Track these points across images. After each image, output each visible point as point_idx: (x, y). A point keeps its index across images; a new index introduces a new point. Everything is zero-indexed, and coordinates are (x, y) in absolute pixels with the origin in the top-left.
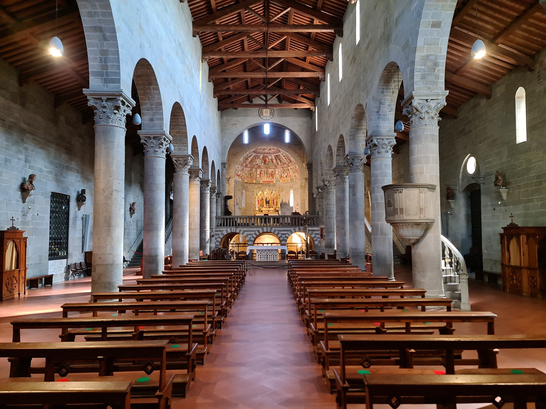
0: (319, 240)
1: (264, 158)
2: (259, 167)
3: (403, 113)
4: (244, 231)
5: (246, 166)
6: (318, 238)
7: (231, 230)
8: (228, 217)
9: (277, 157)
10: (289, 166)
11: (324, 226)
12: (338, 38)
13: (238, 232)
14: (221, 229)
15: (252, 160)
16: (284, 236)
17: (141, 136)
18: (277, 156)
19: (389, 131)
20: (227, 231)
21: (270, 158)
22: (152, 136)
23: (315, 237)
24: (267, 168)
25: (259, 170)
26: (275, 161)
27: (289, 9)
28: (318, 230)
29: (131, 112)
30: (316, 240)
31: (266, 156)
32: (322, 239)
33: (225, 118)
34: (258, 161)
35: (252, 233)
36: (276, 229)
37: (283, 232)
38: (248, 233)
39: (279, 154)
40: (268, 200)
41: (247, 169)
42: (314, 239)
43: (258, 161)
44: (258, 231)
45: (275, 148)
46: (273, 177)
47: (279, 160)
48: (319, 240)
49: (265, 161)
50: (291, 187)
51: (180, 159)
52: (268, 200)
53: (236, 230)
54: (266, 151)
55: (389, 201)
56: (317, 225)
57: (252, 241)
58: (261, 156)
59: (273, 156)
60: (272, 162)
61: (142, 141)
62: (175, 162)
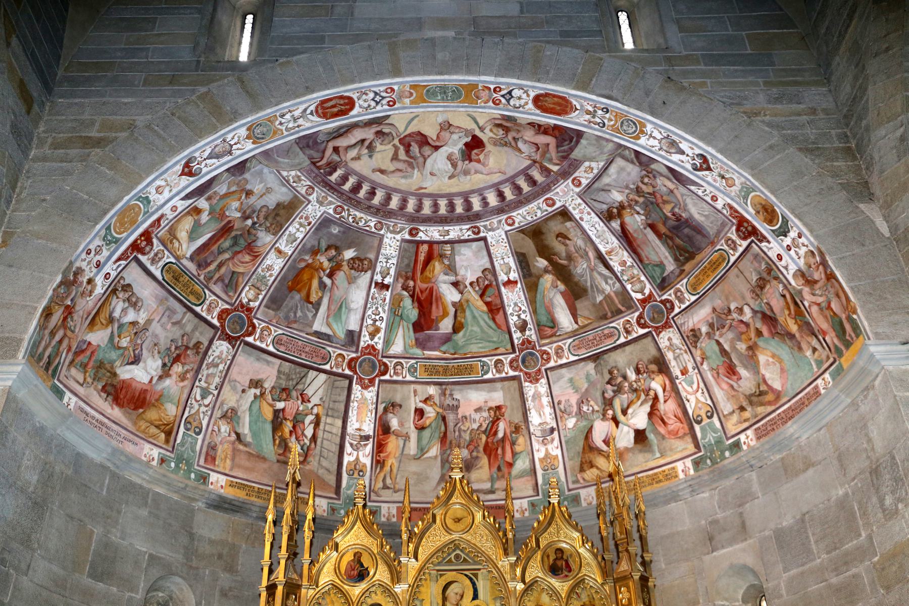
1: (422, 260)
2: (371, 366)
5: (237, 327)
9: (542, 246)
10: (660, 317)
15: (297, 281)
18: (535, 232)
24: (457, 373)
25: (364, 398)
26: (514, 299)
31: (433, 252)
34: (362, 306)
39: (566, 195)
41: (248, 367)
43: (362, 306)
45: (523, 95)
46: (503, 469)
47: (563, 273)
49: (426, 303)
54: (437, 174)
59: (498, 236)
60: (495, 309)
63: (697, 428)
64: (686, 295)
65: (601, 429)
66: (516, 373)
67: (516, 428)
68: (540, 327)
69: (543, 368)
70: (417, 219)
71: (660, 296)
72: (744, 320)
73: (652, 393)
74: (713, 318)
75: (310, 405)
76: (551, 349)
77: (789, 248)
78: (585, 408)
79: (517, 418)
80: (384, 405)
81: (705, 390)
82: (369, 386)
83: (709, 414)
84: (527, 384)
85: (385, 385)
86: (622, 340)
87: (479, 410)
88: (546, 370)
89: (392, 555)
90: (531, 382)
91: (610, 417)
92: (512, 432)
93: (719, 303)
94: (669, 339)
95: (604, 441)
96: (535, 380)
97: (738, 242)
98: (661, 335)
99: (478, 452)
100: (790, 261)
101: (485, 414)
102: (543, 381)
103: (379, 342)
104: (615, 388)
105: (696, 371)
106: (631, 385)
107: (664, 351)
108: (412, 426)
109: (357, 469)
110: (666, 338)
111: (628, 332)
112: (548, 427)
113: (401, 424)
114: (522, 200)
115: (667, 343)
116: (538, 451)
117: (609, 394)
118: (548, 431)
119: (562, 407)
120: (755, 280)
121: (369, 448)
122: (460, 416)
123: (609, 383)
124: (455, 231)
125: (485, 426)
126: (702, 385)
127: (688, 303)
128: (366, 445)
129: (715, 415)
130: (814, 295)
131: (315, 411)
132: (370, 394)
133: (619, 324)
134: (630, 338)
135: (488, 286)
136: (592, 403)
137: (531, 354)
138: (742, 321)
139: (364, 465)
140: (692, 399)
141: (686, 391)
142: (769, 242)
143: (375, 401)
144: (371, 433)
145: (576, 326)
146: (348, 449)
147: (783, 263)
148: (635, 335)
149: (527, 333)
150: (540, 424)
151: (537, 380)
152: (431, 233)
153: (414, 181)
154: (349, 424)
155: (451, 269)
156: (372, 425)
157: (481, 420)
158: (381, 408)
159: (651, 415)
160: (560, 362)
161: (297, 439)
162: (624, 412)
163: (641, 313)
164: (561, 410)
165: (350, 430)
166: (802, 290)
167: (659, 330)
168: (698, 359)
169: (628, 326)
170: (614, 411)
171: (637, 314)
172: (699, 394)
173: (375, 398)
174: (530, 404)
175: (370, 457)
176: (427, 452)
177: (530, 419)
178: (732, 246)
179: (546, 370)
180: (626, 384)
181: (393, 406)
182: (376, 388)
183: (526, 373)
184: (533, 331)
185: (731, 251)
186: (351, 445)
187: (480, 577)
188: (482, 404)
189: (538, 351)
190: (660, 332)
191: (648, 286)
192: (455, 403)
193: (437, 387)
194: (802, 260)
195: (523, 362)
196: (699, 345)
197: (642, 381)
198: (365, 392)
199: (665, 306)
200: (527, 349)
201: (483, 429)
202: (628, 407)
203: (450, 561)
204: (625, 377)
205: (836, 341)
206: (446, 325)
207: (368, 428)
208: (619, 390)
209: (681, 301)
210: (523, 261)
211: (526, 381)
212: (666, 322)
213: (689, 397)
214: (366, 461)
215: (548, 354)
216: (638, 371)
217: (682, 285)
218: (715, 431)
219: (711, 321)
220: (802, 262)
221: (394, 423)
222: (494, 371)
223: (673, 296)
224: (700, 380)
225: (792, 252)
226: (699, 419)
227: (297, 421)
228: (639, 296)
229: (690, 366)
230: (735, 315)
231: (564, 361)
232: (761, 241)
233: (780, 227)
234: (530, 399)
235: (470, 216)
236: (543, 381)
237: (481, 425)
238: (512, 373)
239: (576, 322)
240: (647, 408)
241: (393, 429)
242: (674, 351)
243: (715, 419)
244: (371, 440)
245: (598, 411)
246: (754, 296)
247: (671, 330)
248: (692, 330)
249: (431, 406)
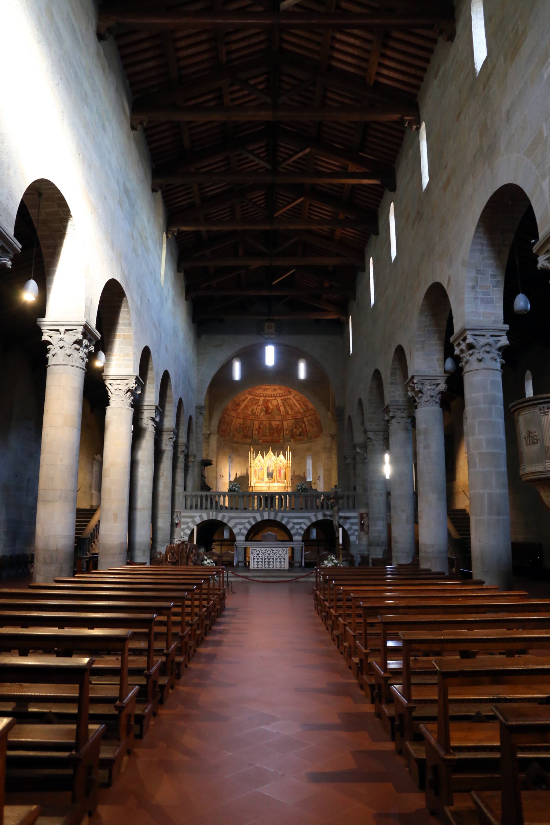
0: (356, 533)
3: (539, 266)
4: (231, 518)
6: (355, 530)
7: (208, 515)
8: (204, 493)
11: (363, 511)
12: (388, 194)
13: (219, 518)
14: (192, 514)
15: (246, 407)
16: (297, 527)
17: (44, 329)
18: (286, 400)
19: (495, 322)
20: (201, 517)
21: (275, 403)
22: (62, 329)
23: (350, 529)
26: (282, 408)
27: (307, 150)
28: (355, 518)
29: (10, 263)
30: (353, 534)
31: (268, 401)
32: (363, 533)
33: (203, 337)
35: (243, 521)
36: (285, 515)
37: (295, 521)
38: (237, 521)
40: (271, 470)
42: (349, 533)
44: (254, 518)
48: (356, 533)
49: (267, 408)
50: (308, 450)
51: (119, 382)
52: (271, 470)
53: (217, 516)
55: (529, 432)
56: (354, 508)
57: (243, 534)
58: (261, 399)
59: (279, 400)
60: (279, 410)
61: (45, 337)
62: (109, 386)
65: (295, 430)
68: (286, 413)
70: (266, 397)
96: (285, 421)
103: (259, 414)
114: (283, 396)
124: (272, 398)
132: (257, 422)
135: (278, 406)
152: (268, 398)
153: (265, 392)
155: (271, 403)
157: (276, 426)
206: (270, 411)
207: (257, 427)
210: (283, 404)
221: (261, 427)
227: (246, 427)
235: (274, 396)
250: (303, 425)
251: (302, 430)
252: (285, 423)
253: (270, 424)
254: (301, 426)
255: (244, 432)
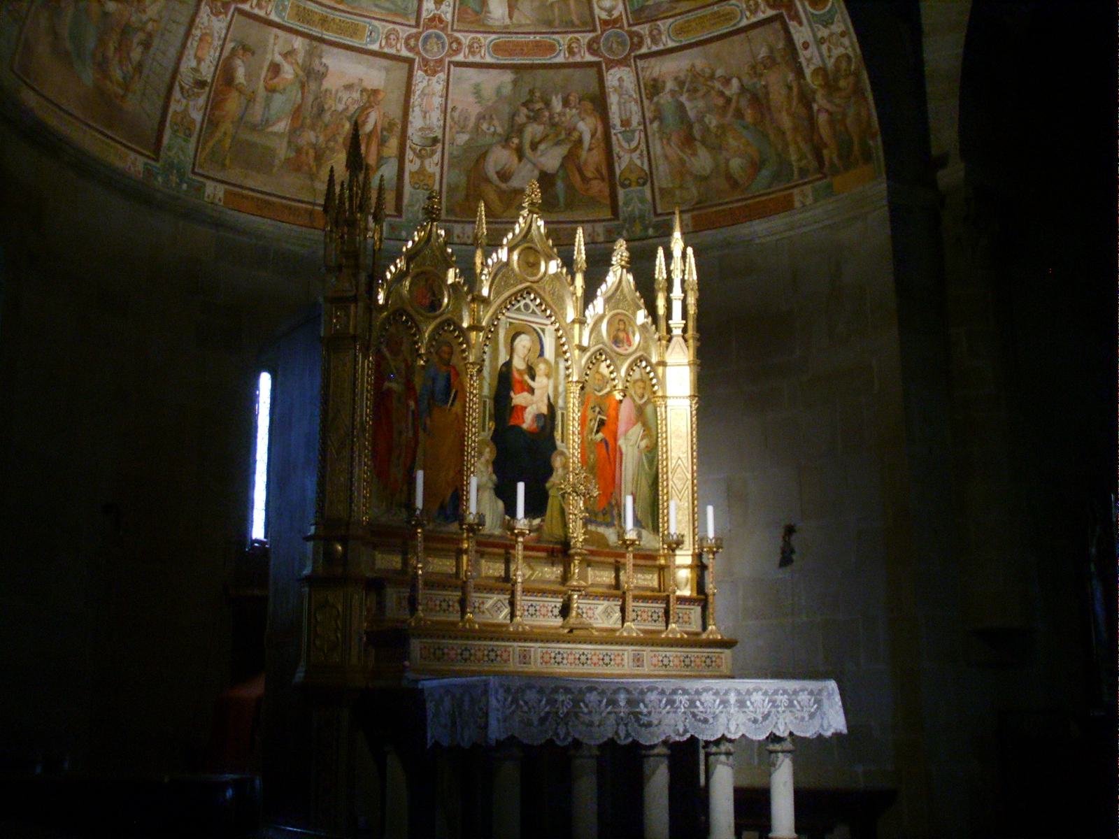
63: (621, 192)
64: (664, 38)
66: (410, 55)
67: (389, 123)
69: (447, 60)
71: (630, 25)
72: (727, 93)
73: (575, 135)
74: (686, 76)
75: (145, 17)
76: (466, 39)
77: (821, 41)
78: (485, 126)
79: (395, 112)
80: (232, 45)
81: (645, 153)
82: (221, 13)
83: (641, 181)
84: (420, 73)
85: (242, 18)
86: (560, 59)
87: (349, 87)
88: (450, 63)
89: (466, 289)
90: (426, 71)
91: (514, 146)
92: (383, 129)
93: (700, 64)
94: (621, 79)
95: (498, 173)
97: (762, 6)
98: (612, 71)
99: (336, 142)
100: (816, 53)
101: (356, 95)
102: (442, 76)
104: (532, 114)
105: (642, 127)
106: (551, 117)
107: (609, 90)
108: (262, 83)
109: (185, 127)
110: (618, 76)
111: (571, 52)
112: (432, 135)
113: (248, 75)
115: (616, 83)
116: (411, 161)
117: (521, 119)
118: (429, 142)
119: (456, 115)
120: (762, 55)
121: (201, 101)
122: (323, 88)
123: (524, 104)
125: (352, 109)
126: (643, 146)
127: (661, 47)
128: (198, 95)
129: (649, 184)
130: (830, 101)
131: (150, 26)
132: (218, 25)
133: (563, 40)
134: (571, 60)
136: (496, 122)
137: (438, 37)
138: (722, 94)
139: (193, 121)
140: (626, 159)
141: (621, 146)
142: (801, 23)
143: (223, 35)
144: (209, 80)
145: (507, 21)
146: (177, 94)
147: (808, 53)
148: (578, 59)
149: (443, 7)
150: (422, 129)
151: (435, 73)
154: (184, 59)
156: (213, 69)
157: (349, 101)
158: (230, 46)
159: (566, 159)
160: (471, 59)
161: (120, 61)
162: (534, 146)
163: (597, 37)
164: (453, 118)
165: (183, 68)
166: (817, 90)
167: (612, 64)
168: (648, 115)
169: (574, 45)
170: (521, 142)
171: (591, 35)
172: (636, 155)
173: (224, 31)
174: (415, 99)
175: (203, 111)
176: (271, 126)
177: (411, 118)
178: (753, 7)
179: (450, 63)
180: (547, 114)
181: (245, 48)
182: (229, 18)
183: (424, 59)
184: (450, 10)
185: (748, 14)
186: (182, 88)
187: (546, 332)
188: (356, 81)
189: (447, 35)
190: (612, 67)
191: (621, 7)
192: (322, 69)
193: (307, 41)
194: (833, 60)
195: (425, 42)
196: (655, 99)
197: (568, 117)
198: (213, 18)
199: (631, 39)
200: (435, 27)
201: (349, 114)
202: (540, 142)
203: (519, 309)
204: (548, 104)
205: (835, 160)
207: (207, 71)
208: (535, 117)
209: (655, 41)
211: (420, 68)
212: (625, 58)
213: (622, 154)
214: (197, 116)
215: (460, 44)
216: (566, 103)
217: (663, 25)
218: (642, 200)
219: (682, 75)
220: (830, 63)
221: (240, 74)
222: (383, 43)
223: (647, 33)
224: (643, 139)
225: (824, 47)
226: (627, 182)
228: (604, 16)
229: (635, 120)
230: (717, 85)
231: (477, 59)
232: (792, 18)
233: (824, 14)
234: (418, 93)
236: (442, 76)
237: (347, 109)
238: (405, 53)
239: (511, 17)
240: (563, 150)
241: (237, 82)
242: (620, 95)
243: (647, 189)
244: (207, 89)
245: (500, 135)
246: (752, 72)
247: (628, 69)
248: (655, 80)
249: (292, 64)
250: (586, 127)
251: (570, 159)
252: (428, 87)
253: (311, 74)
254: (559, 132)
255: (103, 67)
